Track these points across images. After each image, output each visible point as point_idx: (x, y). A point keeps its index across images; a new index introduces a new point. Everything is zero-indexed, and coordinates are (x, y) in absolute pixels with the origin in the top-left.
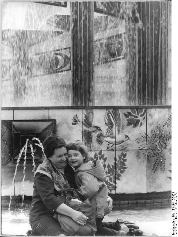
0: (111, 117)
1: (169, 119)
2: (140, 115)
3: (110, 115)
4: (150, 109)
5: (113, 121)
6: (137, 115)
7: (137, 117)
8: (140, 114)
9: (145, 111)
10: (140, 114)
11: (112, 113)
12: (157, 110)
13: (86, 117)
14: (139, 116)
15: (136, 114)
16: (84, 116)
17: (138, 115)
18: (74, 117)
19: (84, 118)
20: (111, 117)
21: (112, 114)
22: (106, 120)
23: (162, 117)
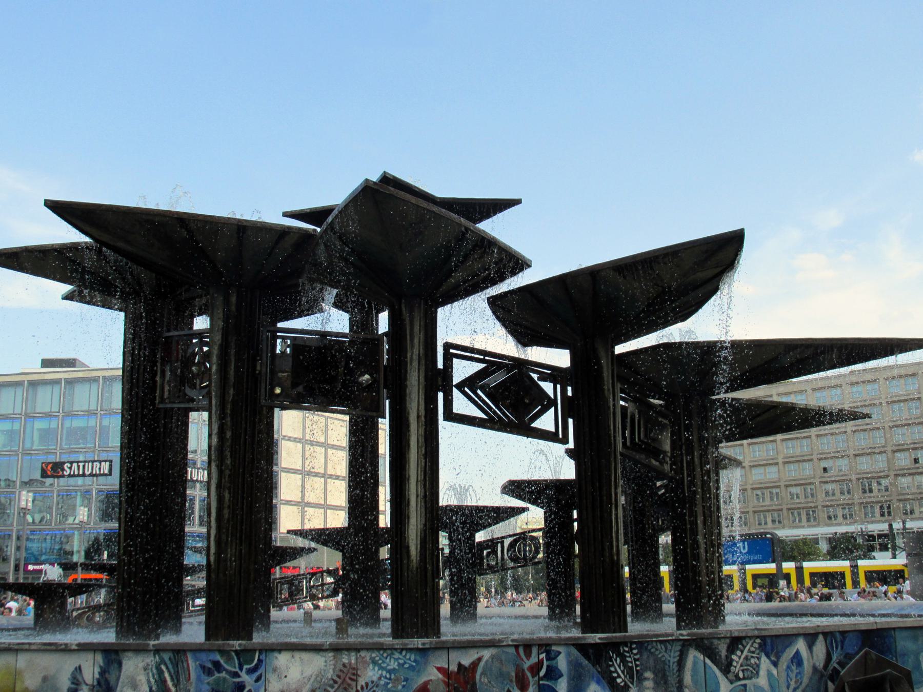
0: (167, 675)
1: (335, 682)
2: (246, 669)
3: (163, 667)
4: (276, 654)
5: (170, 683)
6: (237, 670)
7: (236, 675)
8: (248, 667)
9: (260, 661)
10: (245, 667)
11: (168, 662)
12: (298, 655)
13: (103, 672)
14: (243, 674)
15: (235, 667)
16: (97, 670)
17: (241, 669)
18: (73, 673)
19: (97, 676)
20: (167, 675)
21: (170, 666)
22: (153, 681)
23: (314, 677)
